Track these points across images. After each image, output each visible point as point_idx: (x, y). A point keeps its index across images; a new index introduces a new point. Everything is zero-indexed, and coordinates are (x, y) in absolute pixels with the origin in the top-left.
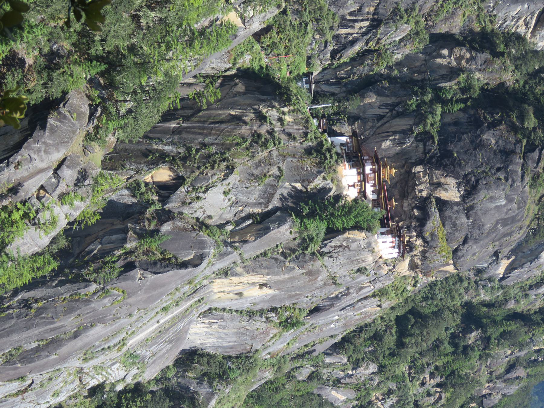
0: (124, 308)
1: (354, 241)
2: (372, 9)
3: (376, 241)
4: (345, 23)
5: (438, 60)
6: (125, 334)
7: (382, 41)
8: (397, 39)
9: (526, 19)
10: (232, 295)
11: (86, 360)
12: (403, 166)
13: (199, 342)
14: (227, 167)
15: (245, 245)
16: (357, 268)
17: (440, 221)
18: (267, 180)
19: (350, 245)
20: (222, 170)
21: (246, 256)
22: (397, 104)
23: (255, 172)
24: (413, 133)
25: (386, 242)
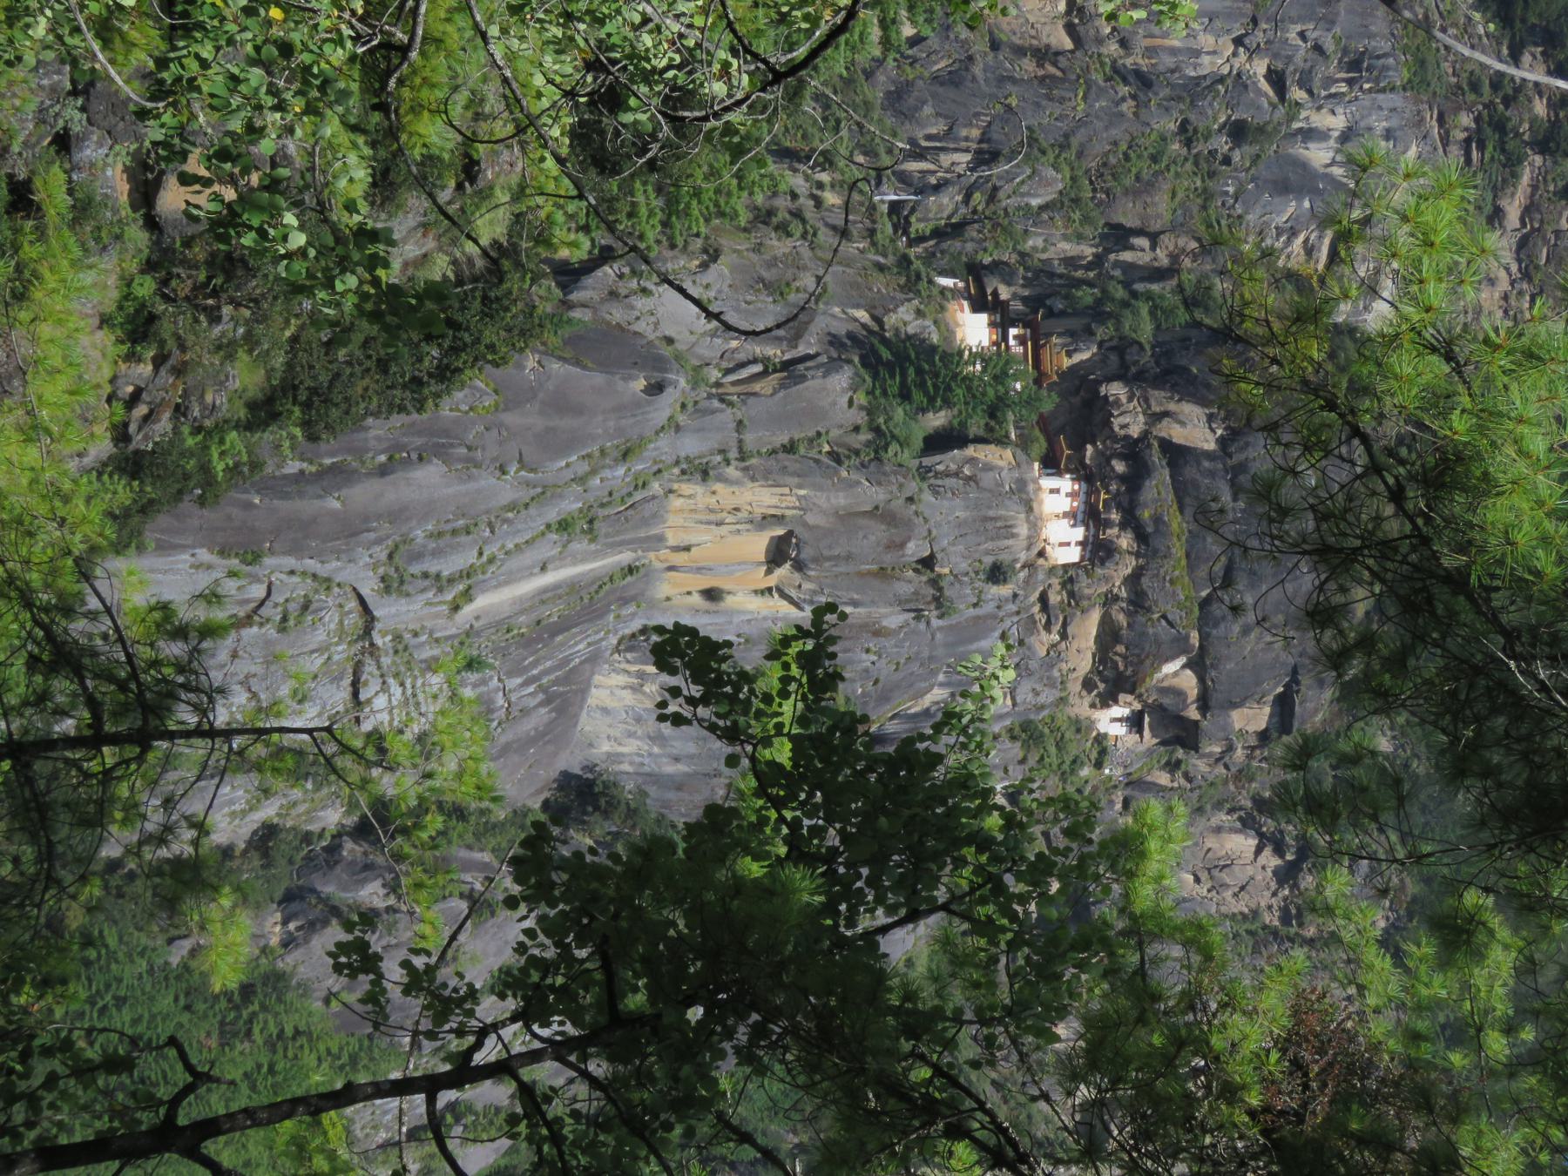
0: (495, 432)
1: (988, 468)
2: (975, 133)
3: (1035, 481)
4: (918, 154)
5: (1127, 256)
6: (475, 553)
7: (1001, 194)
8: (1035, 202)
9: (1306, 241)
10: (696, 599)
11: (388, 586)
12: (1077, 391)
13: (606, 747)
14: (705, 251)
15: (751, 400)
16: (988, 560)
17: (1171, 496)
18: (792, 297)
19: (981, 475)
20: (691, 256)
21: (749, 438)
22: (1049, 296)
23: (766, 274)
24: (1092, 333)
25: (1057, 491)
